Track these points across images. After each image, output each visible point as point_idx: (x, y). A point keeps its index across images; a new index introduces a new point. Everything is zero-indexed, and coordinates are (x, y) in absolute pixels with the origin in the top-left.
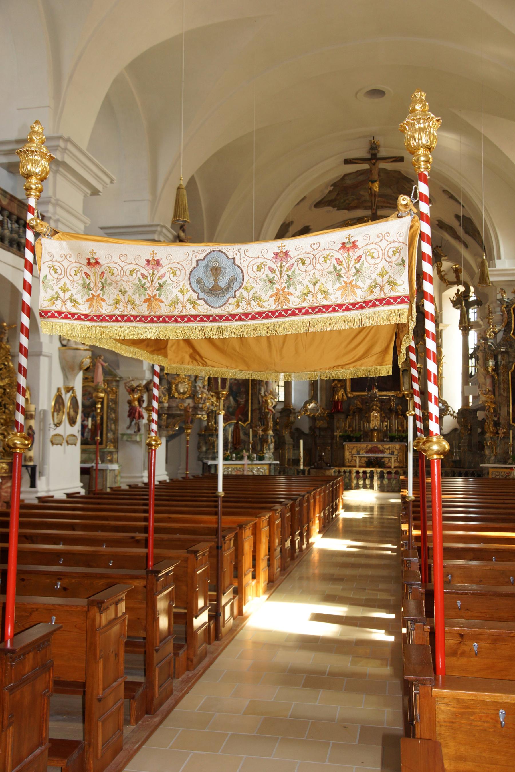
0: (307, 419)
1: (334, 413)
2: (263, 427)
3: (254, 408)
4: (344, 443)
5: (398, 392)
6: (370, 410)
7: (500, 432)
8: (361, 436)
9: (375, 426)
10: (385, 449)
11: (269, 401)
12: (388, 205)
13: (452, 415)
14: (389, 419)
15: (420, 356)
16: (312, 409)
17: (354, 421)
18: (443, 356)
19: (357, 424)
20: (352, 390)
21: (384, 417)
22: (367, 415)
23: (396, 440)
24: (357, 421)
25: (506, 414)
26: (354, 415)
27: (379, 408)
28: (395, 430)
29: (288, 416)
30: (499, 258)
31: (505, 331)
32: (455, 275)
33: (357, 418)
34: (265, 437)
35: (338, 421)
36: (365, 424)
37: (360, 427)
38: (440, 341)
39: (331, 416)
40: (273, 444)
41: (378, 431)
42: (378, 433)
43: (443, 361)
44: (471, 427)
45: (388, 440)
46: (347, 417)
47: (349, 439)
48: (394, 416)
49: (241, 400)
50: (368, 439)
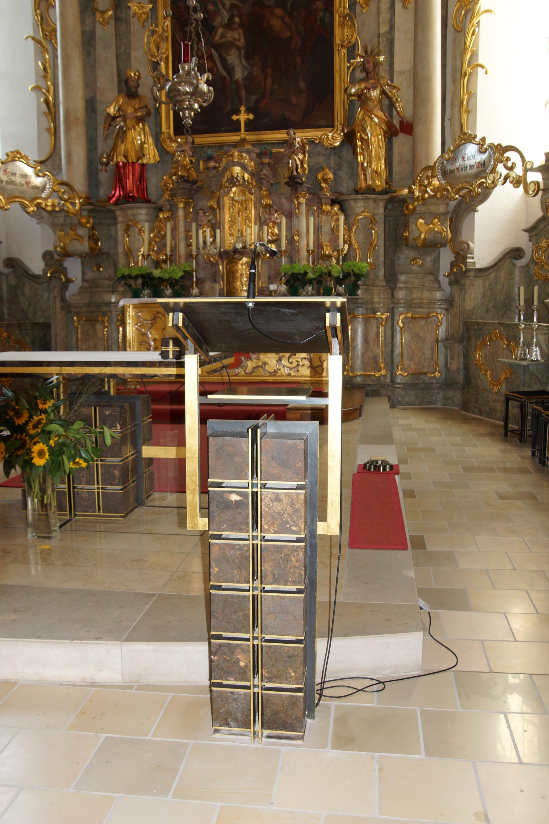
1: (117, 203)
13: (517, 183)
14: (290, 216)
19: (182, 235)
21: (268, 206)
24: (181, 224)
26: (173, 209)
27: (252, 174)
33: (181, 213)
35: (127, 229)
36: (201, 232)
46: (158, 216)
48: (302, 200)
50: (217, 287)
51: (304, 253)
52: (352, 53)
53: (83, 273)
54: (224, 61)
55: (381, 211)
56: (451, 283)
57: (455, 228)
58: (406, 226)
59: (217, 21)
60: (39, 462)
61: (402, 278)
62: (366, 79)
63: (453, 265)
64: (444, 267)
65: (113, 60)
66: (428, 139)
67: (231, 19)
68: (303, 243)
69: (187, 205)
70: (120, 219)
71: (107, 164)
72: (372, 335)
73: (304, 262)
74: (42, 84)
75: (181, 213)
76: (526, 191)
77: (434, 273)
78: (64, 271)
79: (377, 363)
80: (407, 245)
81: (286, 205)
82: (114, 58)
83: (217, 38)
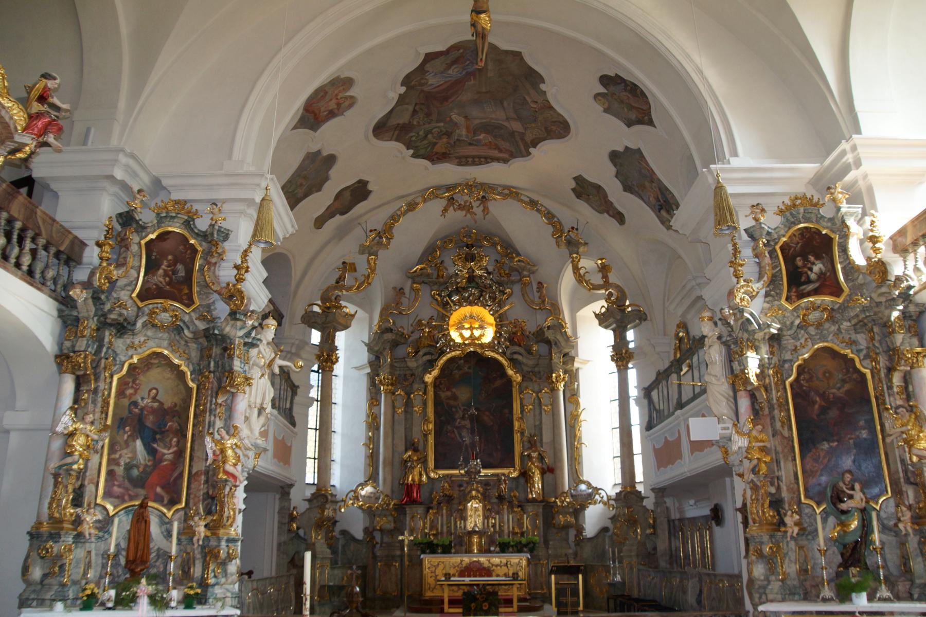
0: (360, 514)
1: (406, 503)
2: (210, 518)
3: (194, 471)
4: (422, 556)
5: (512, 470)
6: (465, 498)
7: (788, 520)
8: (451, 542)
9: (476, 525)
10: (493, 565)
11: (230, 452)
12: (496, 153)
14: (498, 513)
15: (545, 411)
16: (367, 498)
17: (440, 518)
18: (582, 408)
19: (445, 522)
20: (437, 467)
21: (489, 509)
22: (461, 507)
23: (511, 549)
24: (445, 517)
25: (792, 478)
27: (482, 494)
28: (509, 532)
29: (322, 508)
30: (735, 154)
31: (767, 295)
32: (600, 275)
33: (444, 511)
34: (213, 543)
35: (413, 517)
36: (458, 523)
37: (449, 527)
38: (576, 387)
39: (400, 509)
40: (238, 561)
41: (481, 533)
42: (480, 538)
43: (582, 417)
44: (654, 522)
45: (498, 549)
46: (428, 511)
47: (431, 548)
48: (505, 507)
49: (165, 451)
50: (464, 548)
51: (506, 531)
52: (522, 433)
53: (382, 539)
54: (460, 434)
55: (541, 510)
56: (575, 545)
57: (576, 518)
58: (553, 518)
59: (457, 416)
60: (484, 608)
61: (551, 543)
62: (530, 448)
63: (576, 536)
64: (572, 538)
65: (403, 430)
66: (563, 477)
67: (463, 416)
68: (506, 527)
69: (447, 507)
70: (408, 512)
71: (402, 484)
72: (539, 572)
73: (506, 537)
74: (368, 442)
75: (444, 511)
76: (609, 508)
77: (567, 540)
78: (373, 538)
79: (542, 587)
80: (554, 527)
81: (496, 507)
82: (403, 430)
83: (457, 423)
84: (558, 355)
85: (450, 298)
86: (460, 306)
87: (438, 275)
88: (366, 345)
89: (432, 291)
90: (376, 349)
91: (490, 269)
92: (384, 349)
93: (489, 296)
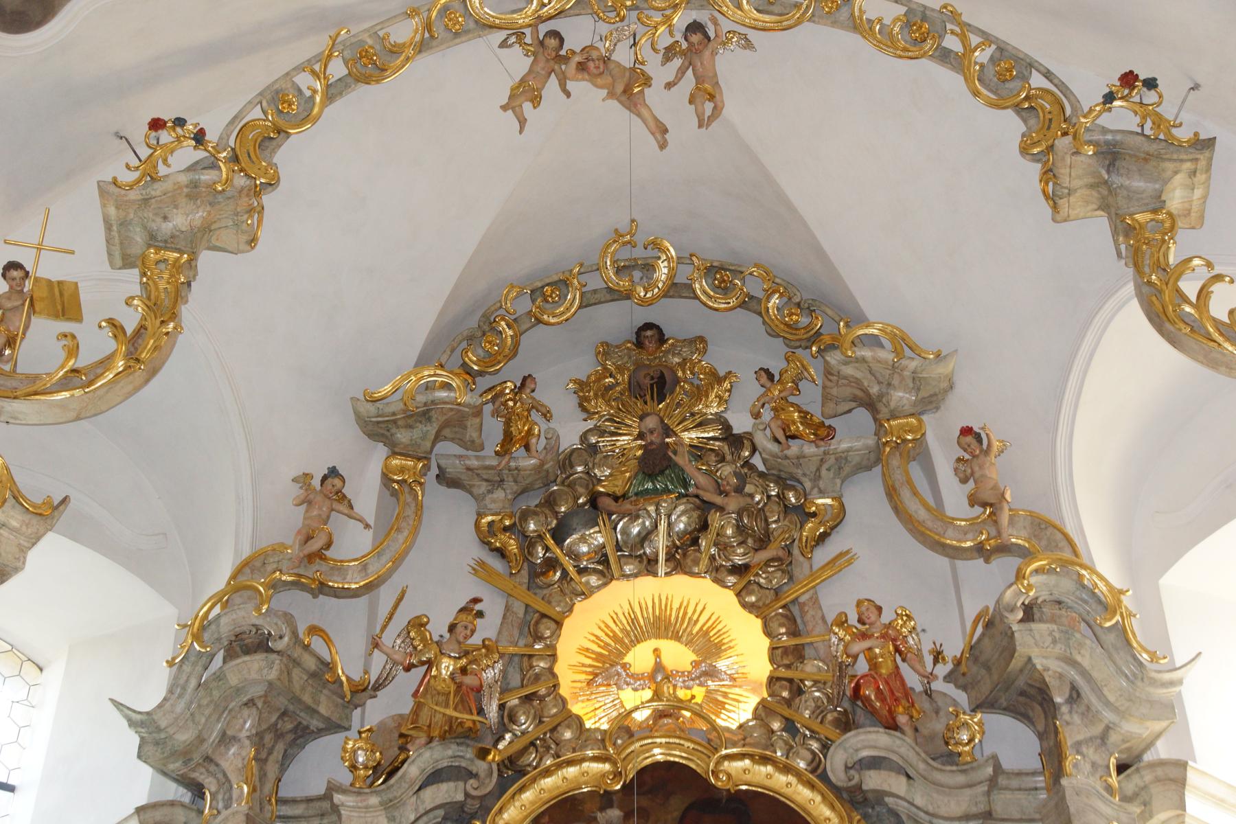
84: (1090, 752)
85: (559, 541)
86: (607, 576)
87: (508, 438)
88: (143, 723)
89: (480, 515)
90: (184, 737)
91: (741, 423)
92: (226, 739)
93: (740, 529)
